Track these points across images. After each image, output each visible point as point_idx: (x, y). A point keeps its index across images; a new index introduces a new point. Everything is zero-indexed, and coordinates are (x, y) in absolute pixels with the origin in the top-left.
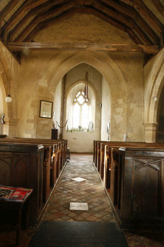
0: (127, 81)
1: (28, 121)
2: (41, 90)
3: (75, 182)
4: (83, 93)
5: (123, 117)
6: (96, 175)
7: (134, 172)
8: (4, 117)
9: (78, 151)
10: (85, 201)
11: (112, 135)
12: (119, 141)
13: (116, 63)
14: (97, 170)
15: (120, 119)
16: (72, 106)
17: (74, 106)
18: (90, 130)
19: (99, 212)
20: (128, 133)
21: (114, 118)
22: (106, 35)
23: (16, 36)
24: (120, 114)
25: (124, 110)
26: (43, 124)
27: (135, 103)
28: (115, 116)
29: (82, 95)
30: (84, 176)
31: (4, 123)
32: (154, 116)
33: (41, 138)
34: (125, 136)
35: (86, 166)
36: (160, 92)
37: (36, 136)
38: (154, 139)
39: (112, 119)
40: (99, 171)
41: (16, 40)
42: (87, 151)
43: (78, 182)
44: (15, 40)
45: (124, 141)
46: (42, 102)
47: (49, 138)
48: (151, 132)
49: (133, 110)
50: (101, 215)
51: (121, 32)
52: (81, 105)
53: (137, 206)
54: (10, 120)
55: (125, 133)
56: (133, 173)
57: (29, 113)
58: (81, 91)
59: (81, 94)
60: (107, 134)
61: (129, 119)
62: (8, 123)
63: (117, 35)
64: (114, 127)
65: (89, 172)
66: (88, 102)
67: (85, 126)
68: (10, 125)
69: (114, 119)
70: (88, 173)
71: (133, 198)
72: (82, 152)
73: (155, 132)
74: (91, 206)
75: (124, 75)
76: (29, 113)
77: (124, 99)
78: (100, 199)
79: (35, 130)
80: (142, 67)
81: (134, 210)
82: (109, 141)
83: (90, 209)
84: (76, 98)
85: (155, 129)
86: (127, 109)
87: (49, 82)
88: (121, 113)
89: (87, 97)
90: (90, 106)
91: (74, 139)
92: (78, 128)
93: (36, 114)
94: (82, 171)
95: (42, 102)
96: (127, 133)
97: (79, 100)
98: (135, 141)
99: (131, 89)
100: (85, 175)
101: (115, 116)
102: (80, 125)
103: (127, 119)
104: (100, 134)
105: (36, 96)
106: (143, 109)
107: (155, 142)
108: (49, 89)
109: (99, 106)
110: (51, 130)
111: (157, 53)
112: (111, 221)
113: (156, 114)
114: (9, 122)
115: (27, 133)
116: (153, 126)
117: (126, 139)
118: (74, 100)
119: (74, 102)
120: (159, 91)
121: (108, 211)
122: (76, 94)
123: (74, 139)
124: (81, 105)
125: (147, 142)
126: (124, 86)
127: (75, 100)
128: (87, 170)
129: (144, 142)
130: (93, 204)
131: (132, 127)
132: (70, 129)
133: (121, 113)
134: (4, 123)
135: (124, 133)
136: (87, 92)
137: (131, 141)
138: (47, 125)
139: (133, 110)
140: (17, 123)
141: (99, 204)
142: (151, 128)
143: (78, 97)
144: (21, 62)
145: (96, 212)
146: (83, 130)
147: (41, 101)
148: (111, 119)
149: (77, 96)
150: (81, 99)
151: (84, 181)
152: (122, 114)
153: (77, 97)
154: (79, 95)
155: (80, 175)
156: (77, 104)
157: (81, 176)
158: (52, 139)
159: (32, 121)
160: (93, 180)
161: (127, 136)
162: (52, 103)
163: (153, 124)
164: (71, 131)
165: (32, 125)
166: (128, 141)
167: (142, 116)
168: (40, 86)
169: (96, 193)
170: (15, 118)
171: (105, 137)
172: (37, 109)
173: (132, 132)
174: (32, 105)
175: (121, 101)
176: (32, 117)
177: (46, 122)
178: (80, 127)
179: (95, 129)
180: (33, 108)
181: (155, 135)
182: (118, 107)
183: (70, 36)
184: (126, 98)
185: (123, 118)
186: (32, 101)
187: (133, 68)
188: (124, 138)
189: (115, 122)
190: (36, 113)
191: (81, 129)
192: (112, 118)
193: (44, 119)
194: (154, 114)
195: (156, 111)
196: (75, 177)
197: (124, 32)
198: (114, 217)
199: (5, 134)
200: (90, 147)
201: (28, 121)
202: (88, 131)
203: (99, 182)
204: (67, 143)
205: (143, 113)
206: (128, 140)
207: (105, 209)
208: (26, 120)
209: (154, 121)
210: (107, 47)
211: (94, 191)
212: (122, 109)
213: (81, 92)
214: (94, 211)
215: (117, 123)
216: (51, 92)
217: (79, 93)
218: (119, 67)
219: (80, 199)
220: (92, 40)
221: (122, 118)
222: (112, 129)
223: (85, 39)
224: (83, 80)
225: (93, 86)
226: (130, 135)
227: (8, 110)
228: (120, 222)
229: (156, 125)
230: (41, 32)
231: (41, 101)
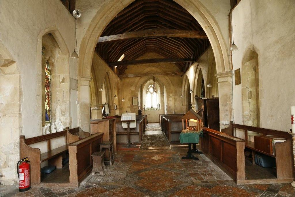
0: (173, 86)
1: (127, 107)
2: (132, 92)
4: (152, 86)
9: (152, 122)
18: (158, 109)
25: (173, 99)
29: (152, 87)
39: (168, 103)
42: (157, 121)
45: (173, 114)
46: (133, 98)
58: (151, 84)
59: (151, 87)
66: (156, 92)
67: (155, 106)
73: (187, 109)
84: (148, 89)
85: (187, 107)
87: (135, 88)
89: (155, 90)
95: (133, 98)
97: (150, 90)
110: (138, 111)
114: (119, 109)
119: (147, 92)
123: (149, 115)
126: (172, 87)
138: (136, 109)
142: (185, 107)
143: (150, 88)
150: (151, 90)
154: (150, 87)
156: (149, 93)
158: (139, 115)
159: (129, 107)
164: (147, 110)
165: (129, 109)
172: (131, 102)
174: (129, 100)
175: (171, 95)
176: (129, 106)
177: (135, 107)
178: (152, 107)
187: (176, 78)
190: (131, 104)
191: (153, 109)
199: (117, 114)
212: (172, 99)
216: (137, 92)
217: (150, 86)
218: (169, 79)
226: (176, 111)
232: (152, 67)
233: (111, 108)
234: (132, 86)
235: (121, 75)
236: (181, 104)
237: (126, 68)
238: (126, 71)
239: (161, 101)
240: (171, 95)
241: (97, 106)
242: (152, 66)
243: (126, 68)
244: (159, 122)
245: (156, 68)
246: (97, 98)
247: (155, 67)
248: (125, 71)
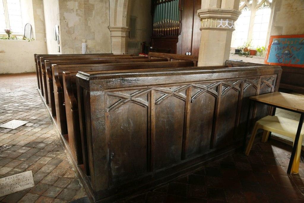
3: (6, 131)
5: (79, 16)
6: (44, 110)
7: (108, 117)
9: (11, 72)
10: (26, 167)
11: (64, 44)
12: (75, 53)
14: (45, 100)
15: (74, 19)
18: (28, 36)
19: (55, 185)
20: (88, 41)
21: (64, 17)
24: (73, 11)
28: (66, 14)
30: (23, 116)
32: (123, 16)
34: (83, 45)
35: (27, 95)
38: (124, 49)
39: (62, 18)
40: (48, 103)
42: (28, 70)
43: (12, 130)
48: (119, 40)
49: (93, 5)
50: (58, 189)
53: (117, 167)
55: (84, 40)
56: (106, 119)
60: (56, 42)
61: (88, 19)
65: (32, 106)
67: (18, 30)
69: (64, 19)
70: (30, 109)
71: (110, 158)
72: (20, 72)
73: (124, 39)
74: (39, 176)
78: (54, 156)
81: (113, 174)
82: (61, 53)
83: (37, 183)
86: (85, 4)
88: (75, 10)
92: (6, 33)
94: (20, 107)
96: (86, 42)
98: (98, 53)
100: (26, 114)
101: (66, 14)
102: (8, 29)
103: (86, 20)
104: (46, 42)
106: (108, 6)
107: (124, 53)
112: (77, 197)
116: (122, 31)
117: (85, 50)
121: (69, 176)
128: (29, 103)
130: (43, 169)
133: (75, 10)
135: (82, 42)
137: (93, 53)
139: (93, 5)
141: (55, 167)
142: (119, 34)
145: (49, 185)
146: (15, 36)
148: (60, 20)
151: (24, 125)
152: (77, 11)
157: (17, 118)
160: (40, 121)
161: (87, 46)
163: (122, 28)
166: (89, 53)
167: (106, 16)
169: (47, 145)
171: (53, 49)
173: (94, 39)
178: (8, 32)
179: (36, 35)
181: (124, 42)
185: (80, 17)
188: (82, 48)
189: (67, 24)
191: (11, 35)
192: (62, 18)
194: (124, 13)
195: (126, 10)
196: (5, 121)
198: (82, 185)
200: (32, 66)
202: (24, 39)
203: (50, 123)
205: (108, 11)
206: (88, 51)
207: (64, 175)
209: (123, 25)
211: (42, 142)
212: (77, 3)
214: (45, 184)
215: (70, 26)
219: (17, 167)
221: (77, 19)
226: (90, 43)
228: (92, 198)
229: (126, 30)
236: (106, 25)
239: (35, 18)
244: (34, 70)
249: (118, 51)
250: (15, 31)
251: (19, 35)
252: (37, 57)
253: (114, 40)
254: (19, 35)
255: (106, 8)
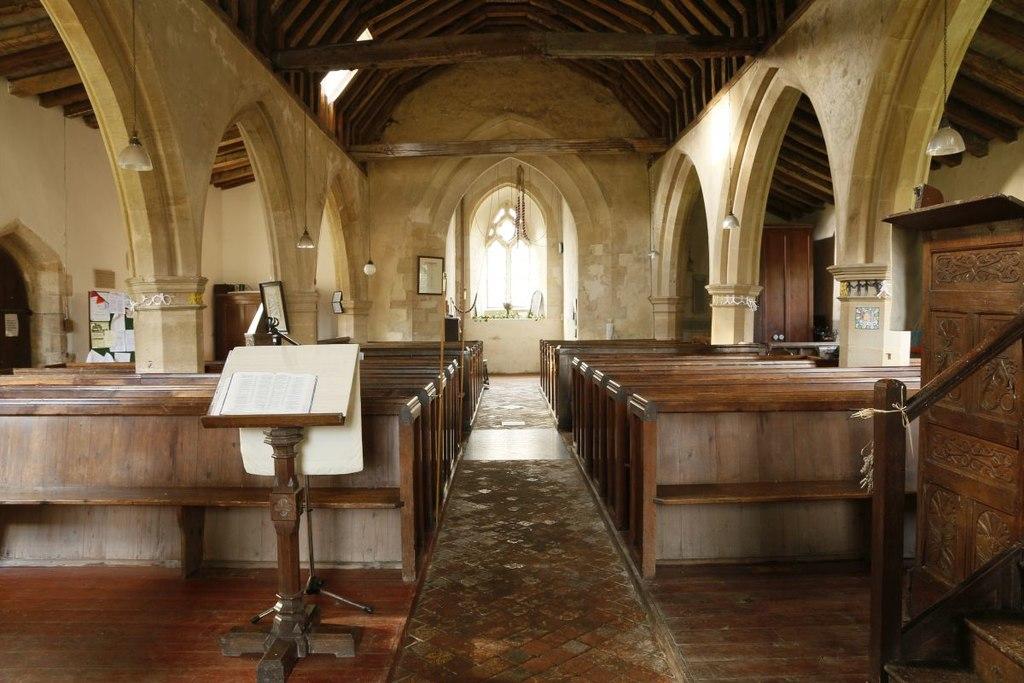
0: (610, 204)
2: (417, 232)
4: (513, 213)
8: (341, 299)
11: (582, 325)
12: (597, 339)
13: (584, 162)
15: (597, 290)
16: (483, 250)
17: (491, 249)
18: (536, 313)
22: (561, 97)
23: (299, 36)
26: (426, 309)
27: (630, 252)
28: (586, 283)
29: (511, 218)
31: (343, 311)
32: (670, 281)
33: (424, 339)
34: (609, 327)
36: (679, 230)
37: (413, 335)
39: (582, 289)
41: (302, 44)
42: (530, 370)
44: (298, 45)
45: (608, 337)
47: (438, 337)
48: (665, 317)
51: (596, 86)
52: (508, 245)
54: (356, 303)
57: (396, 287)
58: (506, 205)
59: (507, 215)
60: (574, 322)
62: (351, 312)
63: (587, 94)
64: (586, 306)
67: (522, 302)
68: (355, 315)
72: (517, 372)
73: (674, 317)
75: (603, 190)
76: (396, 287)
77: (606, 246)
79: (409, 324)
80: (646, 167)
82: (575, 339)
84: (494, 227)
85: (673, 309)
89: (523, 231)
90: (533, 249)
91: (494, 339)
92: (504, 309)
93: (411, 288)
96: (612, 322)
97: (500, 231)
99: (621, 222)
101: (586, 283)
102: (508, 302)
104: (562, 322)
105: (407, 247)
106: (648, 267)
107: (674, 338)
108: (434, 229)
109: (556, 247)
111: (664, 153)
113: (675, 276)
115: (392, 330)
118: (487, 233)
119: (488, 239)
120: (676, 229)
122: (494, 216)
123: (494, 339)
124: (508, 245)
125: (658, 338)
126: (606, 215)
127: (491, 232)
129: (652, 338)
131: (625, 308)
132: (481, 313)
133: (599, 276)
134: (343, 311)
136: (521, 211)
138: (434, 311)
140: (368, 309)
142: (665, 308)
143: (499, 224)
144: (368, 170)
147: (419, 257)
148: (579, 291)
149: (495, 222)
150: (508, 229)
153: (496, 225)
154: (502, 218)
155: (512, 402)
156: (496, 244)
162: (443, 259)
163: (669, 299)
164: (486, 318)
165: (403, 312)
168: (414, 224)
170: (365, 299)
171: (570, 334)
172: (411, 275)
173: (625, 317)
174: (400, 270)
175: (598, 249)
176: (403, 296)
178: (508, 307)
180: (402, 275)
182: (593, 263)
183: (476, 103)
184: (609, 242)
186: (400, 260)
187: (625, 173)
191: (511, 312)
193: (427, 297)
195: (675, 271)
197: (603, 88)
200: (533, 361)
201: (394, 304)
204: (482, 350)
205: (648, 275)
208: (389, 300)
210: (558, 147)
213: (507, 211)
215: (592, 298)
216: (439, 235)
217: (502, 212)
220: (528, 110)
221: (602, 288)
222: (580, 314)
223: (512, 108)
224: (509, 181)
225: (538, 195)
226: (619, 323)
227: (351, 283)
230: (409, 96)
231: (419, 257)
232: (512, 115)
233: (297, 307)
234: (415, 204)
235: (365, 147)
236: (647, 295)
237: (391, 120)
238: (387, 131)
239: (549, 283)
240: (598, 249)
241: (160, 291)
242: (512, 111)
243: (391, 120)
244: (539, 370)
245: (534, 121)
246: (164, 240)
247: (529, 115)
248: (384, 128)
249: (662, 335)
250: (516, 304)
251: (523, 311)
252: (544, 345)
253: (658, 318)
254: (523, 311)
255: (646, 270)
